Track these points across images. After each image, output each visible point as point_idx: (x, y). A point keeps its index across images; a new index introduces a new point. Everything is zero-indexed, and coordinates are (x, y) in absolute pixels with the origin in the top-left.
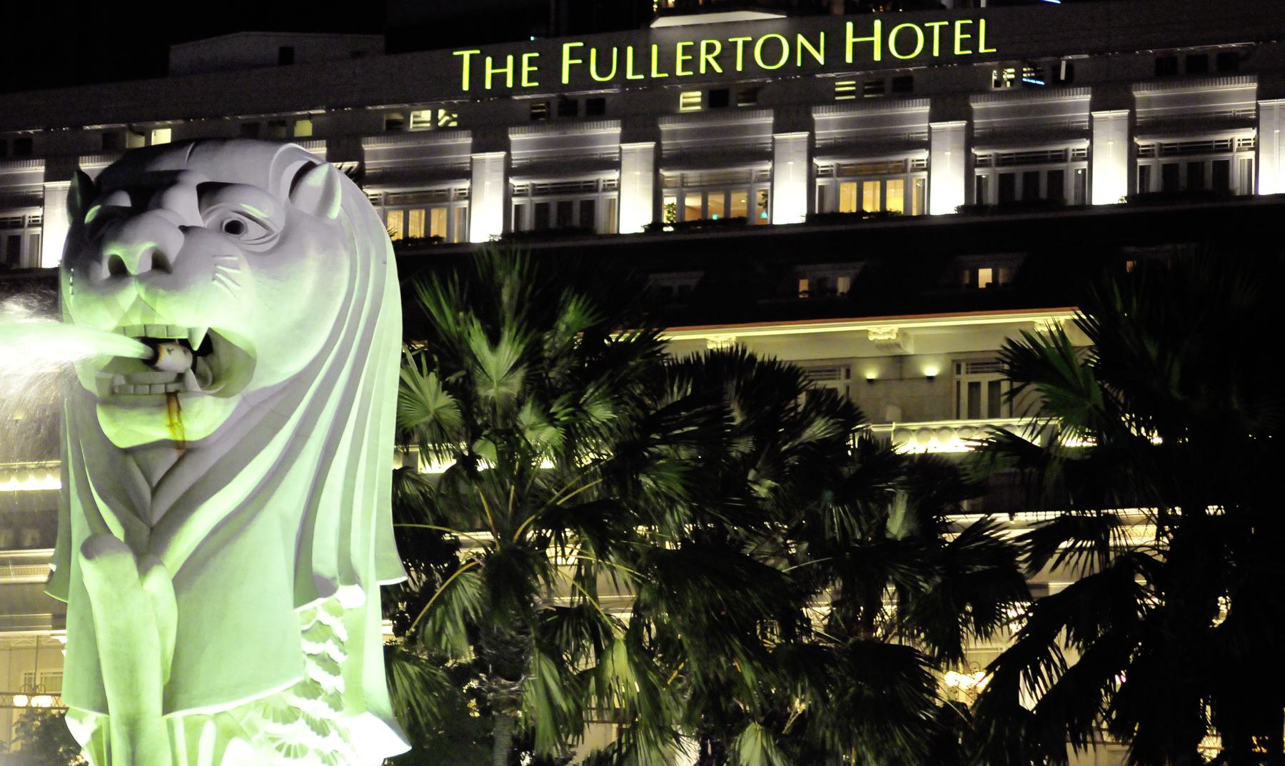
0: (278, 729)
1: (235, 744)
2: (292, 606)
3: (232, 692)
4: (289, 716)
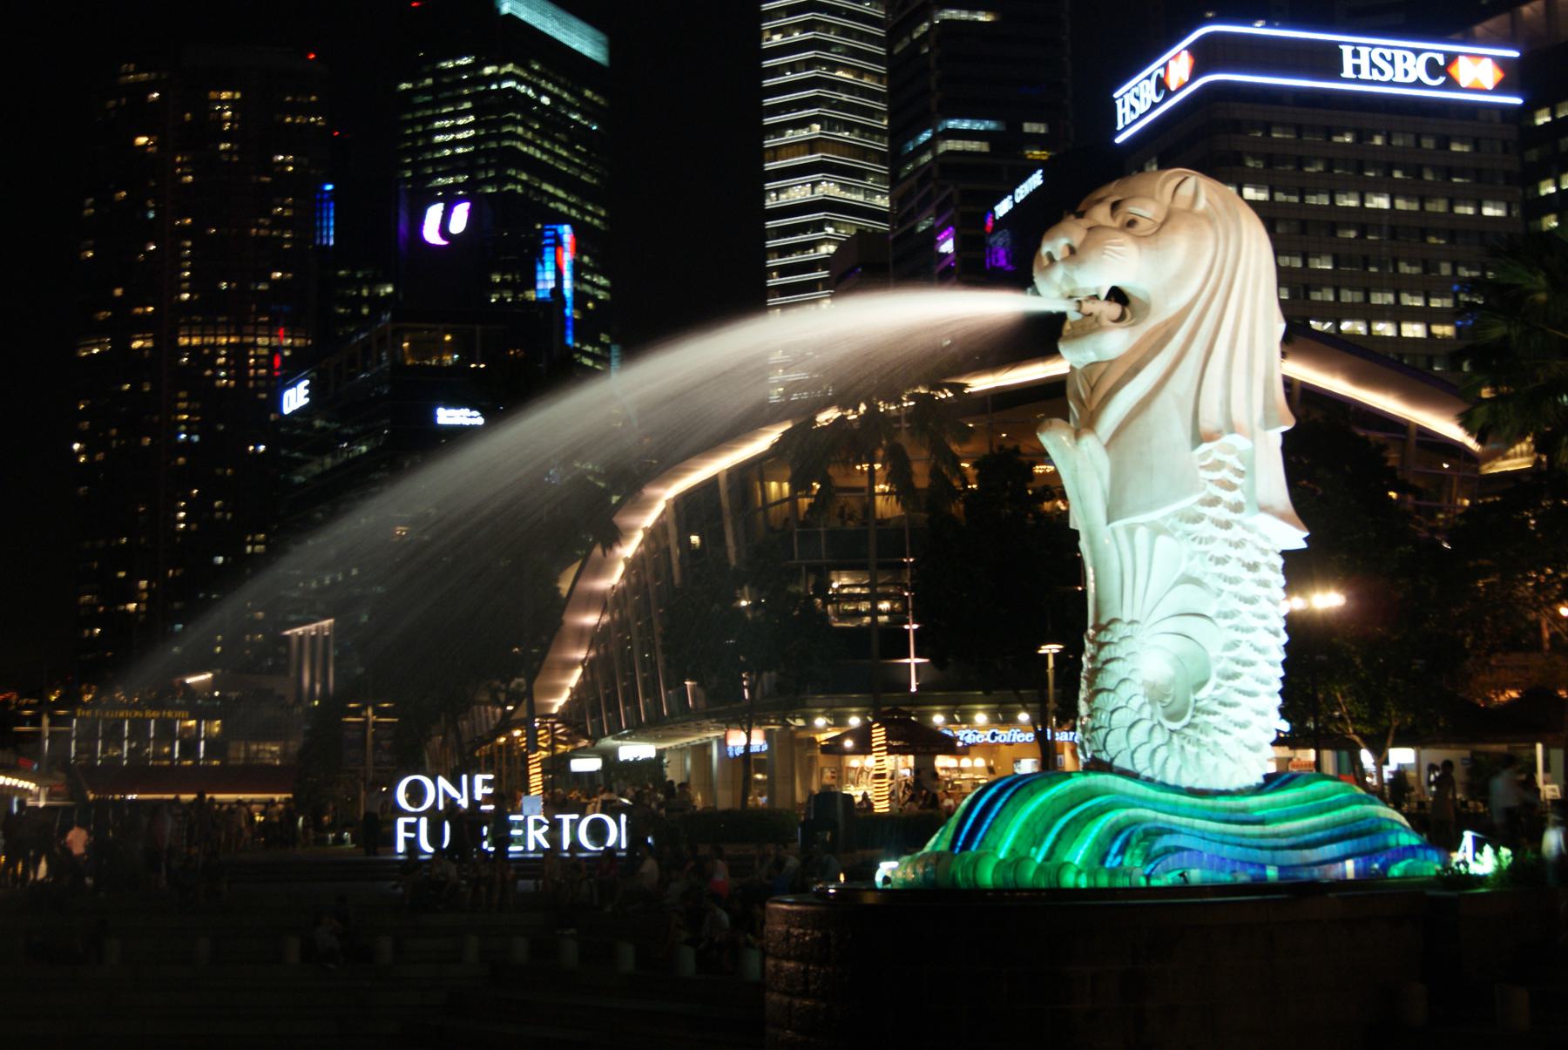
0: (1190, 527)
1: (1162, 540)
3: (1150, 507)
4: (1198, 519)
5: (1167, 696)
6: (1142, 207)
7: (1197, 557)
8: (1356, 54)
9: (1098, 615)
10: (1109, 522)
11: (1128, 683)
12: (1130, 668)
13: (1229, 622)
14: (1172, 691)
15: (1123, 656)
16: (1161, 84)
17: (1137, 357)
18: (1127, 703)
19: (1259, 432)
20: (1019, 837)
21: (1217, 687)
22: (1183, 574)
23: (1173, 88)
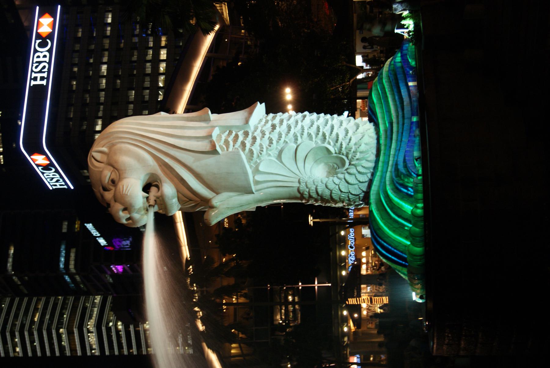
0: (255, 155)
1: (261, 168)
2: (219, 155)
3: (246, 174)
4: (251, 152)
5: (333, 166)
6: (106, 176)
7: (270, 152)
8: (35, 79)
9: (296, 198)
10: (253, 193)
11: (328, 184)
12: (321, 183)
13: (299, 138)
14: (331, 164)
15: (315, 186)
16: (46, 168)
17: (175, 179)
18: (337, 185)
19: (211, 124)
20: (400, 235)
21: (329, 143)
22: (277, 159)
23: (48, 162)
